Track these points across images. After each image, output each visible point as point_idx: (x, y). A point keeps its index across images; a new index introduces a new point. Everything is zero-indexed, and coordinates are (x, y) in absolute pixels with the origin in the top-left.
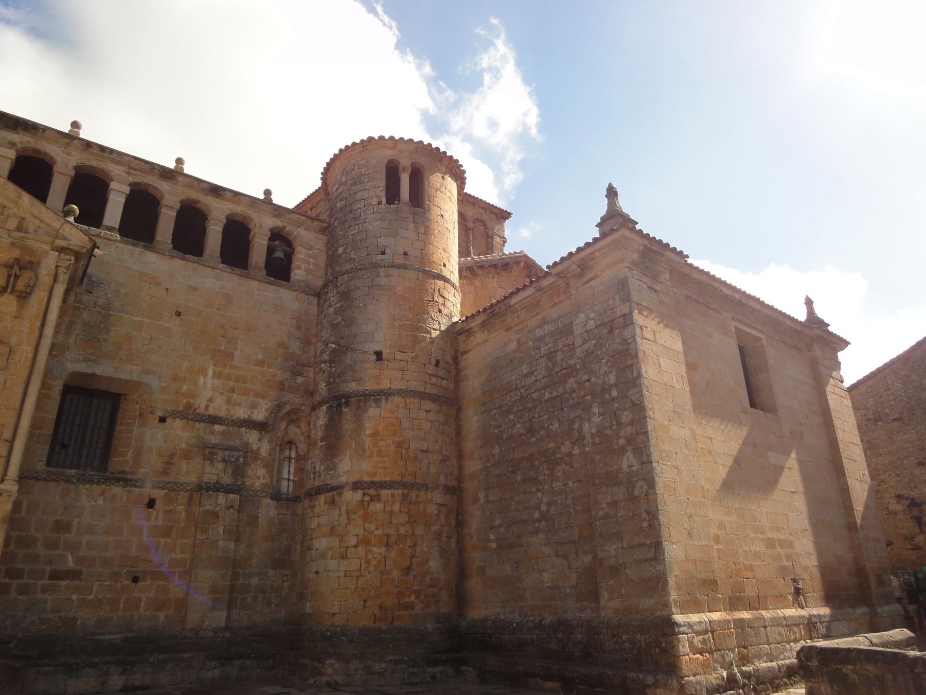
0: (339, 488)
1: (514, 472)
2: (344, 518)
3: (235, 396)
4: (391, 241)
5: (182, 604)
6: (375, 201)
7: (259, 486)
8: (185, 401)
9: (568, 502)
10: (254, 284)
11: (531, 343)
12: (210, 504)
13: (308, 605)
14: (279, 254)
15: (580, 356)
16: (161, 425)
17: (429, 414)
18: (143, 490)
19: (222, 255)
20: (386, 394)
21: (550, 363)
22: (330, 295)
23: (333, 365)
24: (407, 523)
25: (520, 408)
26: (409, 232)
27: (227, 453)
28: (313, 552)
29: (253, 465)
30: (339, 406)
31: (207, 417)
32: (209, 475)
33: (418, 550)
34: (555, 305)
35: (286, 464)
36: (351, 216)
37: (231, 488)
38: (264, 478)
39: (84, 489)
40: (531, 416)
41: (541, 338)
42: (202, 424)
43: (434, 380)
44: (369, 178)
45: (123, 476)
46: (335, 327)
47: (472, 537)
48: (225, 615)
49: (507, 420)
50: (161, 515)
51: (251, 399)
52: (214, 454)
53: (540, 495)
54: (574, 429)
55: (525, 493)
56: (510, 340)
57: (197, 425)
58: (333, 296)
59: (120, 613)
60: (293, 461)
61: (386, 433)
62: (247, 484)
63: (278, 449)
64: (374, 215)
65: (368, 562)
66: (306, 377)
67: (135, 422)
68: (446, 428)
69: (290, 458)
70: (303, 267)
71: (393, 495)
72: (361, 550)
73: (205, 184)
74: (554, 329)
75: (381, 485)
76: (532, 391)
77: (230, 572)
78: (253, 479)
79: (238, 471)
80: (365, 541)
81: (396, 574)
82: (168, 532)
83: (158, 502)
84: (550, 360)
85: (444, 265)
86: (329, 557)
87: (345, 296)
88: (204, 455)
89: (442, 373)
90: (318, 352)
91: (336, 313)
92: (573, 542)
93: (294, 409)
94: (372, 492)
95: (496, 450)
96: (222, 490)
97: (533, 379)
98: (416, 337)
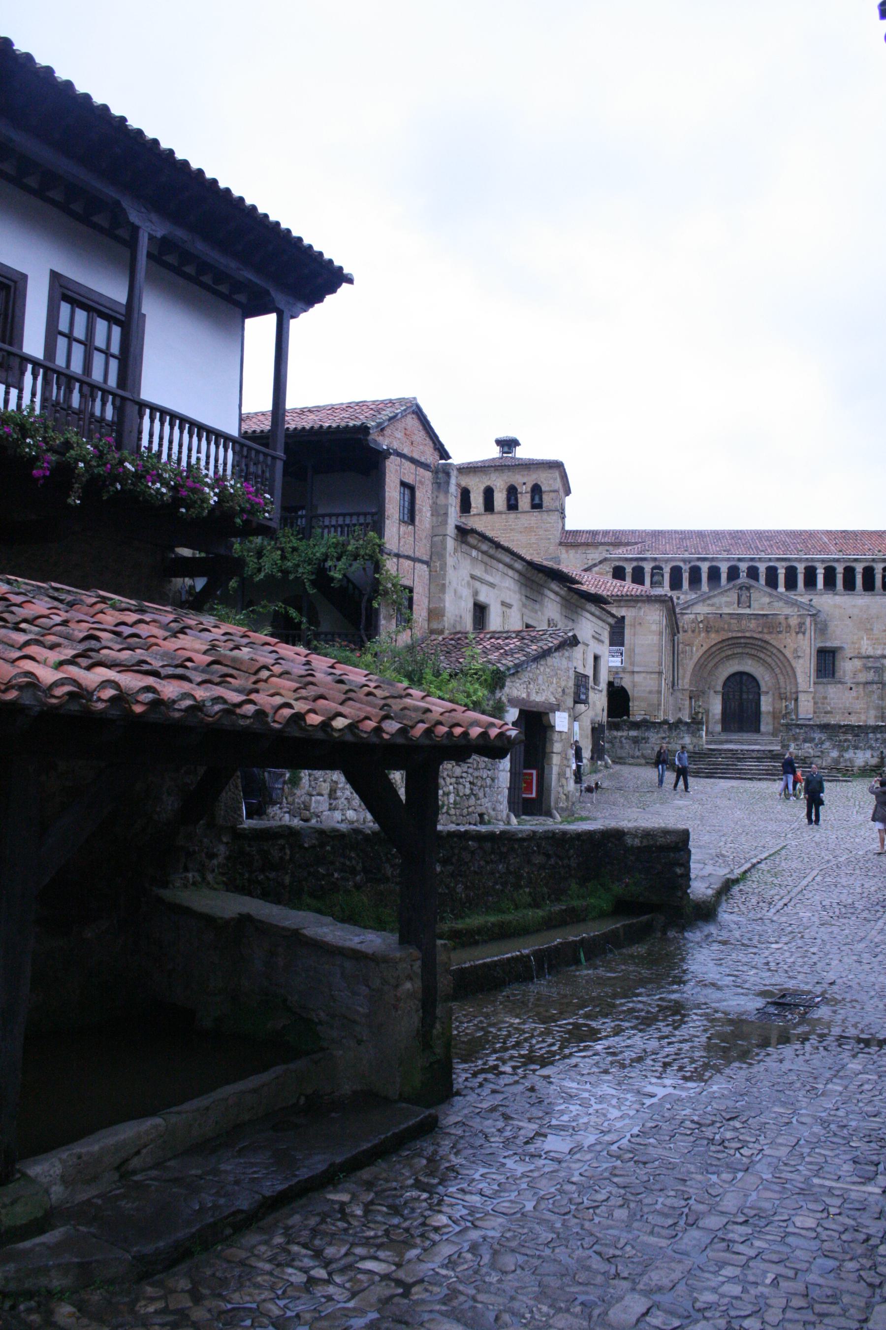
10: (878, 597)
39: (829, 686)
82: (858, 699)
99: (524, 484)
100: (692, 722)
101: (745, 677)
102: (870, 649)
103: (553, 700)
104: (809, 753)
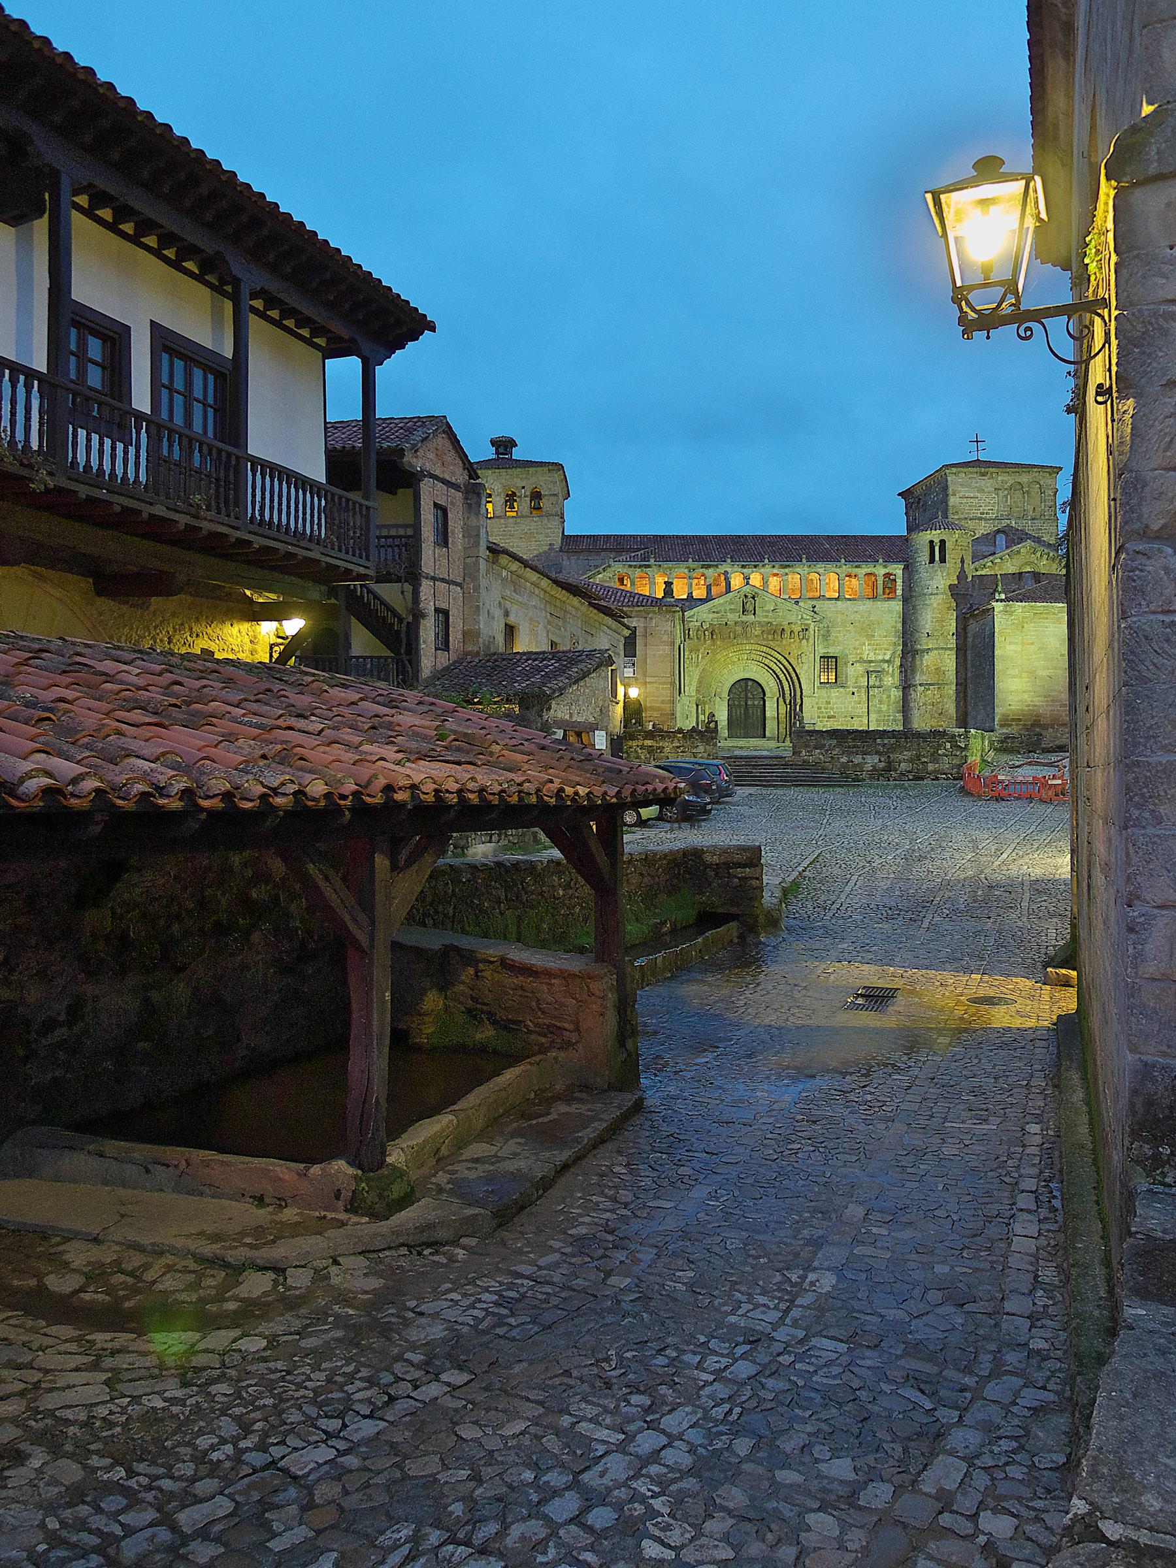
4: (931, 582)
99: (523, 488)
100: (706, 731)
101: (750, 683)
102: (872, 654)
103: (592, 720)
104: (820, 759)
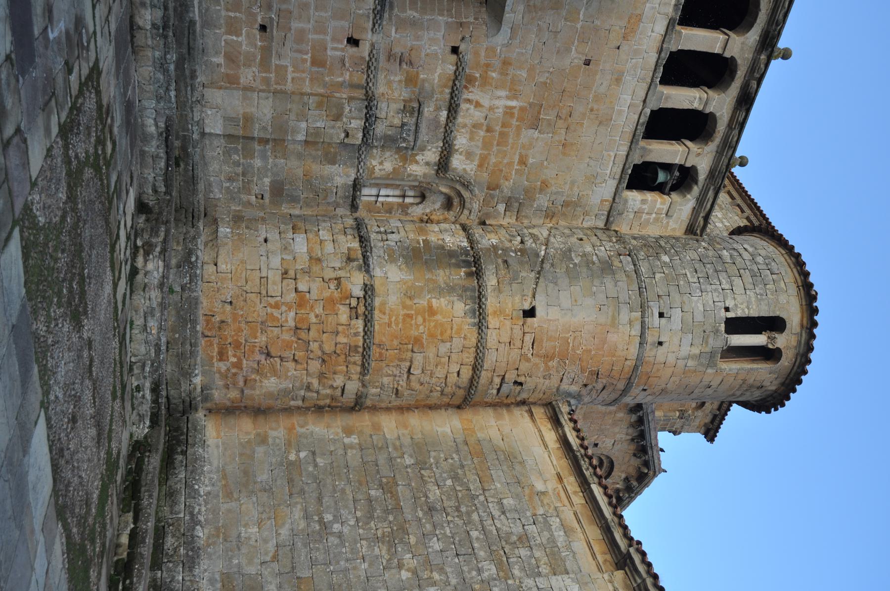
0: (366, 267)
1: (381, 486)
2: (329, 274)
3: (482, 133)
5: (232, 81)
6: (730, 303)
7: (371, 164)
8: (478, 75)
9: (342, 563)
10: (623, 152)
11: (541, 511)
12: (351, 110)
13: (228, 230)
14: (662, 177)
15: (523, 585)
16: (449, 49)
17: (456, 375)
18: (370, 33)
19: (661, 110)
20: (481, 325)
21: (514, 538)
22: (608, 245)
23: (519, 254)
24: (324, 353)
25: (460, 495)
26: (689, 348)
27: (413, 128)
28: (290, 235)
29: (397, 157)
30: (467, 264)
31: (457, 103)
32: (386, 108)
33: (291, 365)
34: (590, 547)
35: (397, 192)
36: (711, 272)
37: (370, 135)
38: (380, 170)
40: (449, 510)
41: (549, 527)
42: (448, 96)
43: (497, 381)
44: (761, 295)
45: (387, 8)
46: (567, 254)
47: (302, 427)
48: (218, 132)
49: (445, 475)
50: (338, 53)
51: (478, 152)
52: (412, 113)
53: (352, 523)
54: (431, 572)
55: (355, 501)
56: (545, 481)
57: (448, 91)
58: (605, 249)
59: (223, 13)
60: (400, 200)
61: (432, 324)
62: (375, 151)
63: (417, 184)
64: (711, 302)
65: (277, 306)
66: (505, 214)
67: (452, 18)
68: (436, 394)
69: (404, 196)
70: (644, 207)
71: (356, 334)
72: (291, 296)
73: (755, 86)
74: (559, 545)
75: (368, 321)
76: (480, 511)
77: (269, 137)
78: (380, 157)
79: (390, 142)
80: (302, 300)
81: (262, 339)
83: (355, 49)
84: (520, 539)
85: (645, 390)
86: (285, 257)
87: (607, 268)
88: (411, 100)
89: (505, 389)
90: (535, 231)
91: (584, 255)
92: (293, 568)
93: (464, 202)
94: (361, 309)
95: (408, 461)
96: (367, 124)
97: (496, 513)
98: (552, 358)
102: (477, 115)
